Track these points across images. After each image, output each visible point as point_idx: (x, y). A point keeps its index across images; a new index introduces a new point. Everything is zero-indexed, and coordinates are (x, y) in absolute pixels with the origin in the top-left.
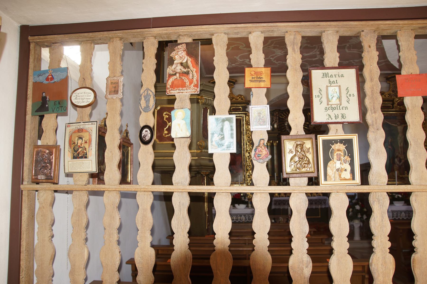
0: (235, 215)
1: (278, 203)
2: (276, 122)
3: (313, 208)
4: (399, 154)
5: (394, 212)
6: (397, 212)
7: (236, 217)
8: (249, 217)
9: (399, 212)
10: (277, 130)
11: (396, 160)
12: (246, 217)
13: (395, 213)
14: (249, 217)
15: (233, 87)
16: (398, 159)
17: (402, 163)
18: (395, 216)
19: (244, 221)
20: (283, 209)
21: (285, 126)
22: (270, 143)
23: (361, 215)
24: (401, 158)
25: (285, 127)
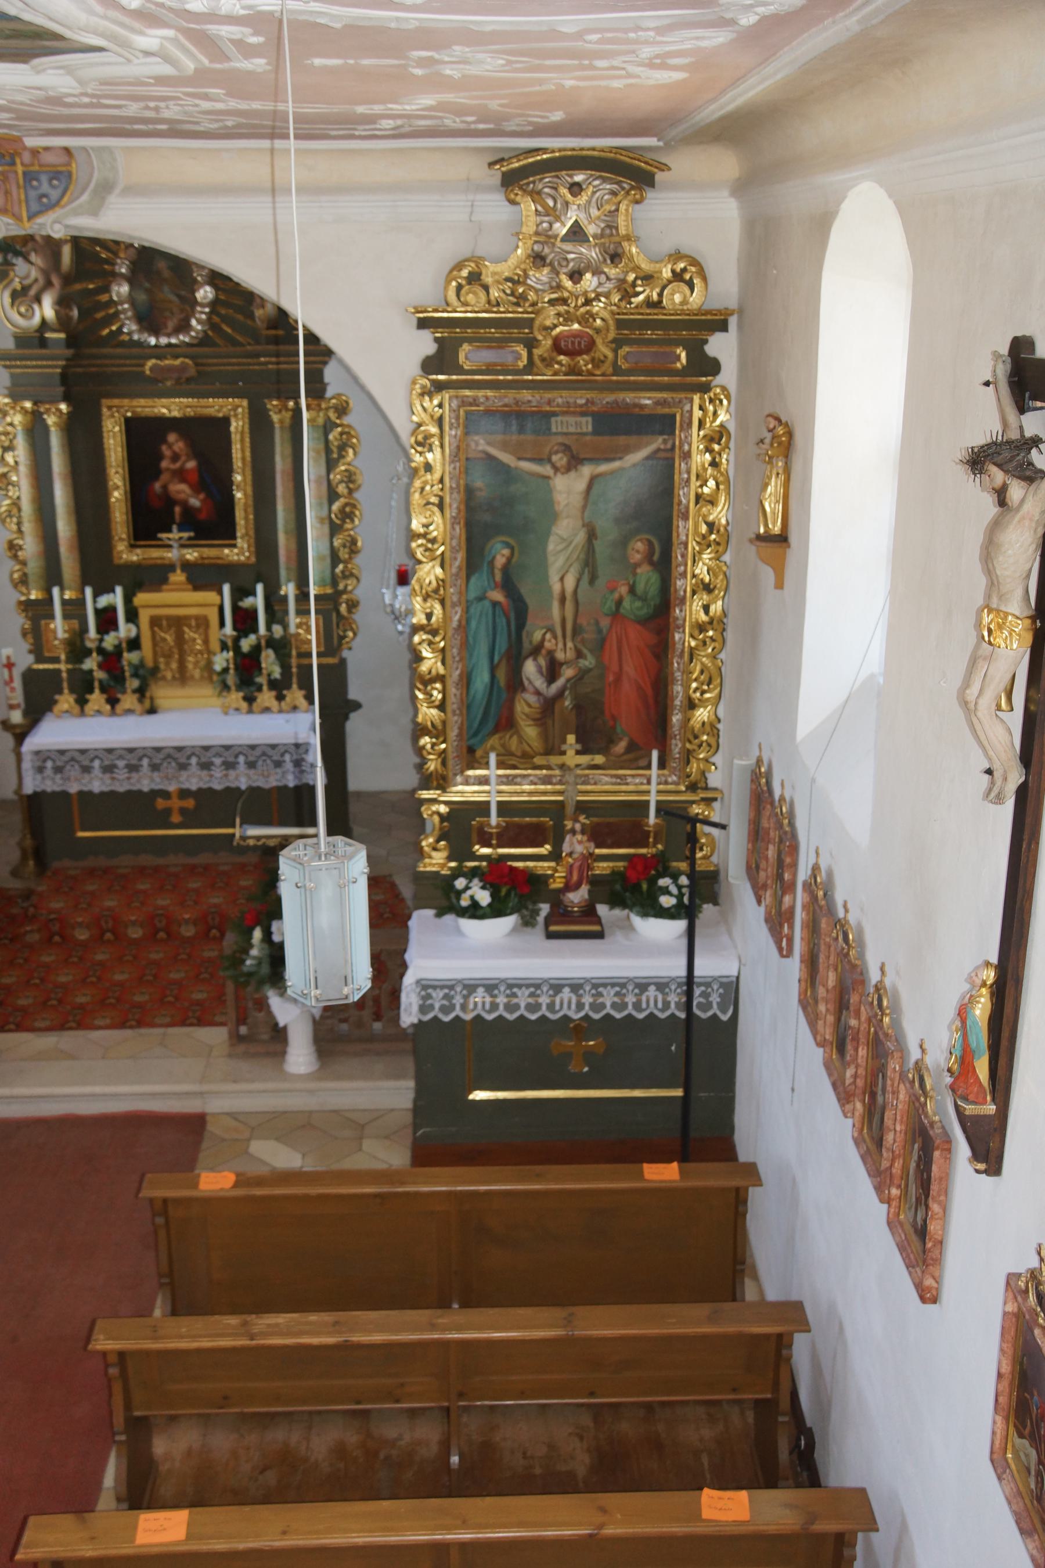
1: (49, 764)
2: (49, 284)
3: (238, 789)
4: (548, 636)
5: (434, 987)
6: (451, 988)
9: (459, 989)
10: (62, 336)
11: (530, 668)
13: (438, 995)
16: (542, 661)
17: (560, 683)
18: (437, 1006)
20: (81, 793)
21: (111, 303)
22: (24, 411)
24: (560, 656)
25: (117, 314)
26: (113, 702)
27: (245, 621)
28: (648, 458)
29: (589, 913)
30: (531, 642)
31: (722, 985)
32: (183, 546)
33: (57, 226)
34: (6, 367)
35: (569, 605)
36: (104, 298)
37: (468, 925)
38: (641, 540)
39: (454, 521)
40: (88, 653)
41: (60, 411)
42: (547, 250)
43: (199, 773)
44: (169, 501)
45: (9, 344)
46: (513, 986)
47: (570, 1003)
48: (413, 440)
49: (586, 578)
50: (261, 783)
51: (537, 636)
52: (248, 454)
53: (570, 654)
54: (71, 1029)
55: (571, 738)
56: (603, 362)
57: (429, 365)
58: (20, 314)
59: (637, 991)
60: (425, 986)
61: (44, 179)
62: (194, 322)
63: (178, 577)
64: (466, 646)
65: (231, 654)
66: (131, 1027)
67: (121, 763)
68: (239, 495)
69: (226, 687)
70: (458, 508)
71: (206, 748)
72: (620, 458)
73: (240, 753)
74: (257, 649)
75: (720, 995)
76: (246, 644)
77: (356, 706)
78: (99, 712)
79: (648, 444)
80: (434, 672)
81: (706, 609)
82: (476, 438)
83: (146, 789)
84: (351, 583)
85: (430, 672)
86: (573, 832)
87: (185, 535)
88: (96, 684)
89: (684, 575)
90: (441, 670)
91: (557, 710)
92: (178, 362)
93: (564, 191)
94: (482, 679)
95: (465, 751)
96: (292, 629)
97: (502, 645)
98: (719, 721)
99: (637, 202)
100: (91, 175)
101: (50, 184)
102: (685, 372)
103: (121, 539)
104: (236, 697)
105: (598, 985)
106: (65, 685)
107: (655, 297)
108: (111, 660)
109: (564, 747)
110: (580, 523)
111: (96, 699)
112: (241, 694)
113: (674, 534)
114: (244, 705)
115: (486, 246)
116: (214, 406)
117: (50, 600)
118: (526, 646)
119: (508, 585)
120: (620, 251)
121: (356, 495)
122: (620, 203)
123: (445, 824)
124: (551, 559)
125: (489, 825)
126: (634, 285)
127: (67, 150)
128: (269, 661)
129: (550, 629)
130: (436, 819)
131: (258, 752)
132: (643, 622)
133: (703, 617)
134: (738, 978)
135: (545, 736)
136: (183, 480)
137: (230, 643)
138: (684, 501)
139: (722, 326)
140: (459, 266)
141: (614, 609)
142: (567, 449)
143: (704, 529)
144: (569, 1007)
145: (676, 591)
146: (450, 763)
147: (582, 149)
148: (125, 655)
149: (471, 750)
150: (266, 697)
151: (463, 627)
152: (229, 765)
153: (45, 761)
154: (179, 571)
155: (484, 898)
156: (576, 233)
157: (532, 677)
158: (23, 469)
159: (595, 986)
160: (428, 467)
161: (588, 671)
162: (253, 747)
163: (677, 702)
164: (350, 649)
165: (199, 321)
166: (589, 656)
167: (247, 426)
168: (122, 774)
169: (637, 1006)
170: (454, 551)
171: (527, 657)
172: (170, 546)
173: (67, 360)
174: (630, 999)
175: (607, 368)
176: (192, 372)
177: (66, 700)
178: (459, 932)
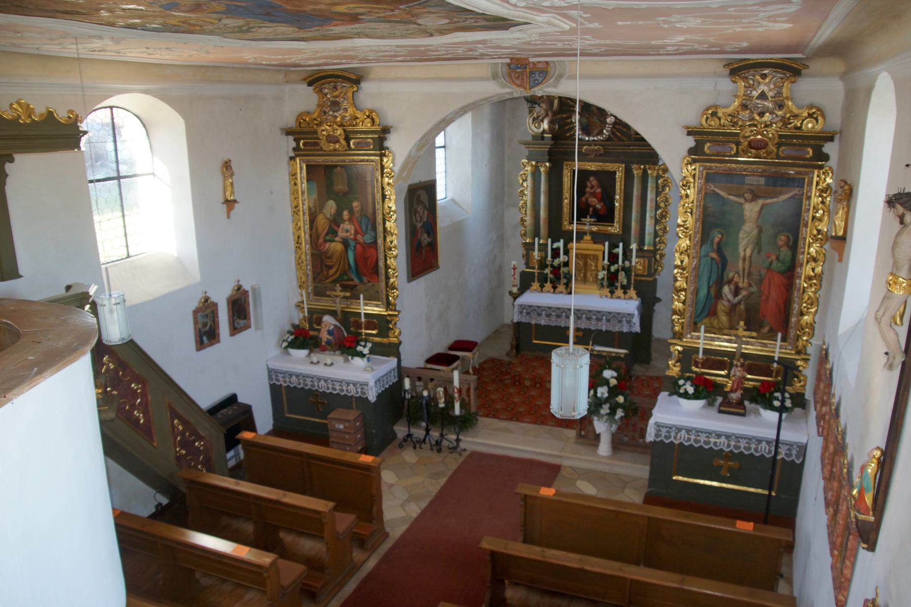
0: (338, 382)
1: (525, 311)
2: (547, 115)
3: (602, 330)
4: (736, 276)
5: (663, 427)
6: (670, 428)
7: (340, 385)
8: (362, 389)
9: (674, 429)
10: (550, 135)
11: (726, 289)
12: (356, 389)
13: (664, 430)
14: (362, 389)
15: (355, 89)
16: (732, 287)
17: (740, 297)
18: (663, 435)
19: (354, 395)
20: (536, 324)
23: (610, 408)
24: (741, 285)
26: (555, 288)
27: (613, 258)
28: (790, 198)
29: (740, 404)
30: (728, 277)
31: (798, 446)
32: (591, 225)
33: (540, 92)
34: (527, 148)
35: (747, 262)
36: (569, 121)
37: (683, 401)
38: (784, 235)
39: (697, 220)
40: (547, 266)
41: (546, 166)
42: (748, 103)
43: (586, 321)
44: (588, 205)
45: (530, 139)
46: (699, 431)
47: (724, 443)
48: (681, 184)
49: (756, 251)
50: (611, 329)
51: (731, 275)
52: (623, 187)
53: (746, 285)
54: (514, 421)
55: (742, 323)
56: (771, 153)
57: (691, 151)
58: (535, 127)
59: (757, 443)
60: (659, 426)
61: (537, 73)
62: (605, 131)
63: (588, 237)
64: (698, 276)
65: (606, 272)
66: (538, 424)
67: (554, 314)
68: (617, 204)
69: (603, 286)
70: (699, 215)
71: (590, 311)
72: (777, 197)
73: (604, 315)
74: (617, 271)
75: (797, 451)
76: (613, 269)
77: (659, 300)
78: (549, 291)
79: (791, 191)
80: (682, 287)
81: (813, 270)
82: (710, 184)
83: (563, 326)
84: (662, 246)
85: (680, 287)
86: (737, 366)
87: (593, 220)
88: (549, 280)
89: (803, 253)
90: (685, 287)
91: (737, 309)
92: (596, 147)
93: (758, 77)
94: (703, 292)
95: (692, 323)
96: (633, 264)
97: (714, 277)
98: (815, 323)
99: (793, 82)
100: (555, 72)
101: (540, 76)
102: (811, 159)
103: (566, 220)
104: (606, 291)
105: (738, 437)
106: (536, 279)
107: (799, 125)
108: (556, 270)
109: (738, 327)
110: (756, 225)
111: (548, 286)
112: (608, 290)
113: (800, 234)
114: (609, 295)
115: (721, 101)
116: (610, 167)
117: (534, 244)
118: (725, 279)
119: (719, 250)
120: (783, 104)
121: (668, 208)
122: (784, 82)
123: (680, 355)
124: (740, 240)
125: (699, 358)
126: (789, 119)
127: (547, 63)
128: (622, 277)
129: (737, 273)
130: (677, 352)
131: (612, 315)
132: (782, 273)
133: (812, 274)
134: (806, 444)
135: (730, 320)
136: (595, 197)
137: (606, 267)
138: (806, 219)
139: (831, 139)
140: (707, 109)
141: (768, 265)
142: (752, 191)
143: (815, 232)
144: (724, 445)
145: (799, 260)
146: (685, 328)
147: (767, 59)
148: (562, 268)
149: (695, 324)
150: (619, 292)
151: (697, 268)
152: (599, 320)
153: (523, 309)
154: (588, 235)
155: (691, 390)
156: (763, 96)
157: (727, 294)
158: (529, 189)
159: (737, 438)
160: (687, 196)
161: (753, 293)
162: (610, 313)
163: (795, 312)
164: (659, 275)
165: (607, 131)
166: (754, 286)
167: (623, 175)
168: (553, 318)
169: (756, 450)
170: (695, 233)
171: (725, 284)
172: (585, 224)
173: (551, 145)
174: (753, 446)
175: (773, 155)
176: (602, 152)
177: (536, 285)
178: (679, 404)
